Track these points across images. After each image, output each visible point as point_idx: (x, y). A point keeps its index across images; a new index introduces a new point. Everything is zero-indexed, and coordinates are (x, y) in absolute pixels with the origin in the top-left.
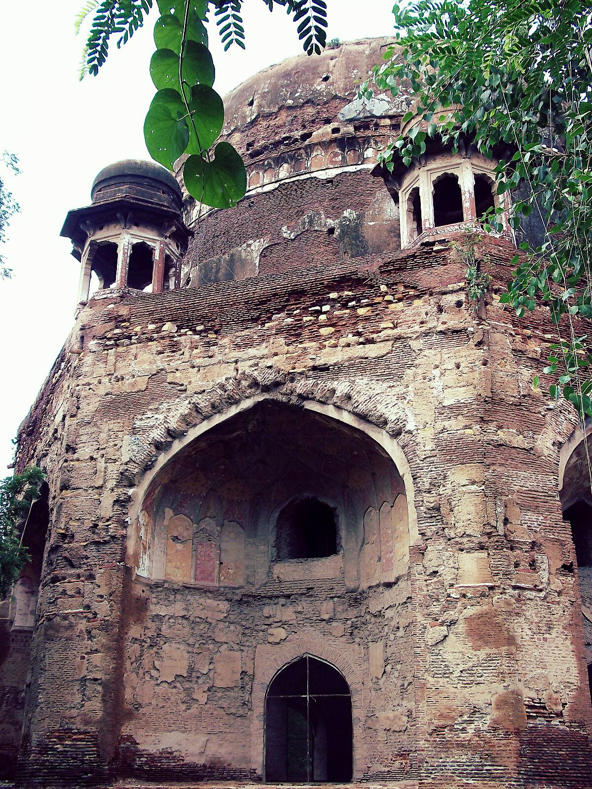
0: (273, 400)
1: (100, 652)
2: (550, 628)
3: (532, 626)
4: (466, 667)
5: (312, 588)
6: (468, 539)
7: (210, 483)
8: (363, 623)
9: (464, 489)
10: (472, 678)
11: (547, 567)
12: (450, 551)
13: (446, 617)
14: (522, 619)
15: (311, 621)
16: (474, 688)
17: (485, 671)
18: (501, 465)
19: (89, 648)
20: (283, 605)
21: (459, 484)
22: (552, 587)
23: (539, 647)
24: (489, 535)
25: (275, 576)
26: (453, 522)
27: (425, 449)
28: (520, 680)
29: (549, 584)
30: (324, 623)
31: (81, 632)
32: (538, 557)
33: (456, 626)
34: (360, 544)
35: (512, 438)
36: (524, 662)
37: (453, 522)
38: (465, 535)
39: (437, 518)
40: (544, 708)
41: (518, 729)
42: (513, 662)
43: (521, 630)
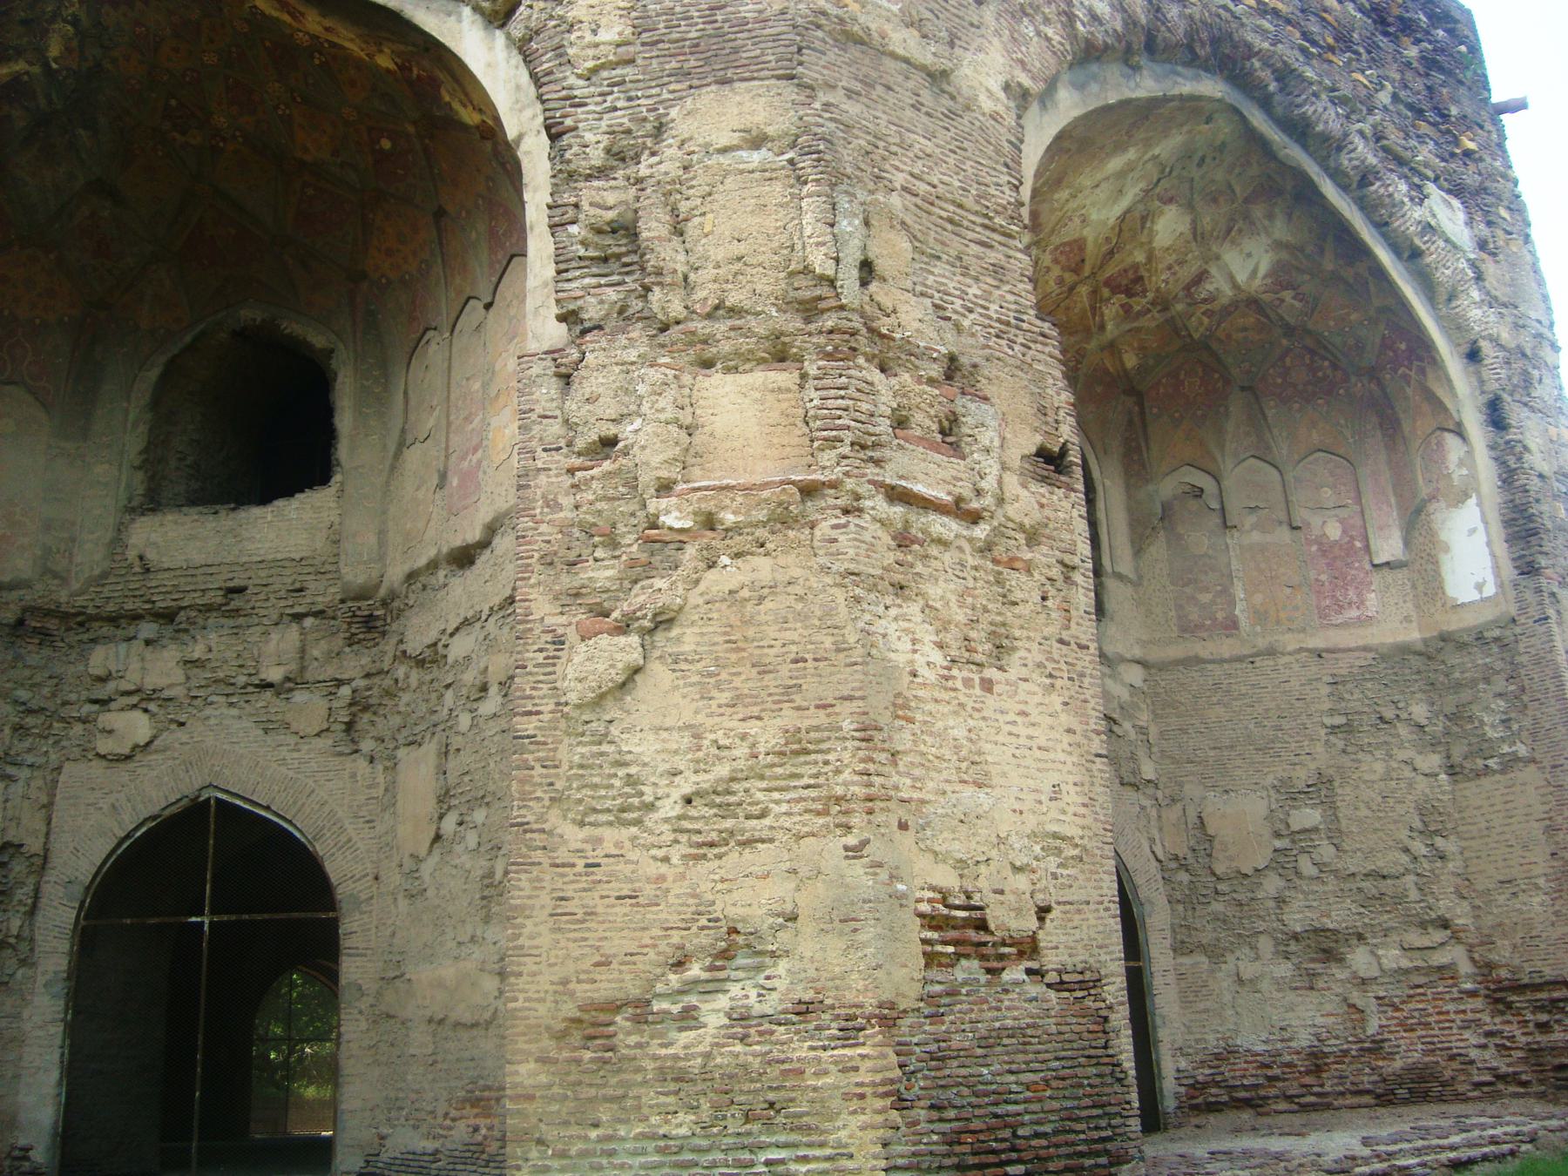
2: (1001, 649)
3: (948, 638)
4: (705, 780)
5: (240, 590)
6: (729, 323)
8: (388, 693)
9: (725, 160)
10: (729, 824)
11: (997, 443)
12: (667, 366)
13: (641, 599)
14: (914, 609)
15: (230, 690)
16: (735, 859)
17: (776, 795)
18: (851, 94)
20: (148, 643)
21: (708, 145)
22: (1011, 510)
23: (969, 708)
24: (809, 310)
25: (132, 554)
26: (681, 268)
27: (597, 39)
28: (903, 826)
29: (1001, 501)
30: (268, 694)
32: (971, 412)
33: (675, 632)
34: (392, 448)
35: (888, 27)
36: (918, 759)
37: (681, 268)
38: (721, 312)
39: (625, 260)
40: (982, 926)
41: (892, 1006)
42: (883, 757)
43: (909, 646)
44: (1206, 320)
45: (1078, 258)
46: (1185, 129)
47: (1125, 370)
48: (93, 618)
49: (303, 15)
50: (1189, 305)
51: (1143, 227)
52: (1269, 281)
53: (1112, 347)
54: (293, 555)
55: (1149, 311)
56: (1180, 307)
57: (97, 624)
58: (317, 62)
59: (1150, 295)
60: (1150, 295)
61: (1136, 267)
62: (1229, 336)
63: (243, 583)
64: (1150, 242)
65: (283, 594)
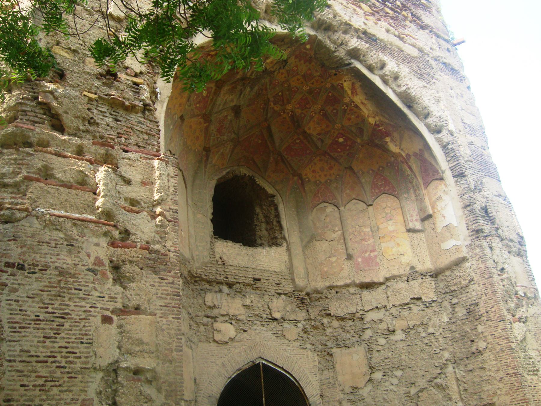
0: (320, 41)
1: (145, 312)
7: (187, 107)
19: (119, 300)
20: (228, 294)
25: (217, 256)
30: (275, 323)
31: (99, 262)
34: (306, 240)
48: (203, 280)
49: (357, 94)
54: (275, 270)
57: (204, 283)
58: (343, 108)
63: (260, 277)
65: (274, 284)
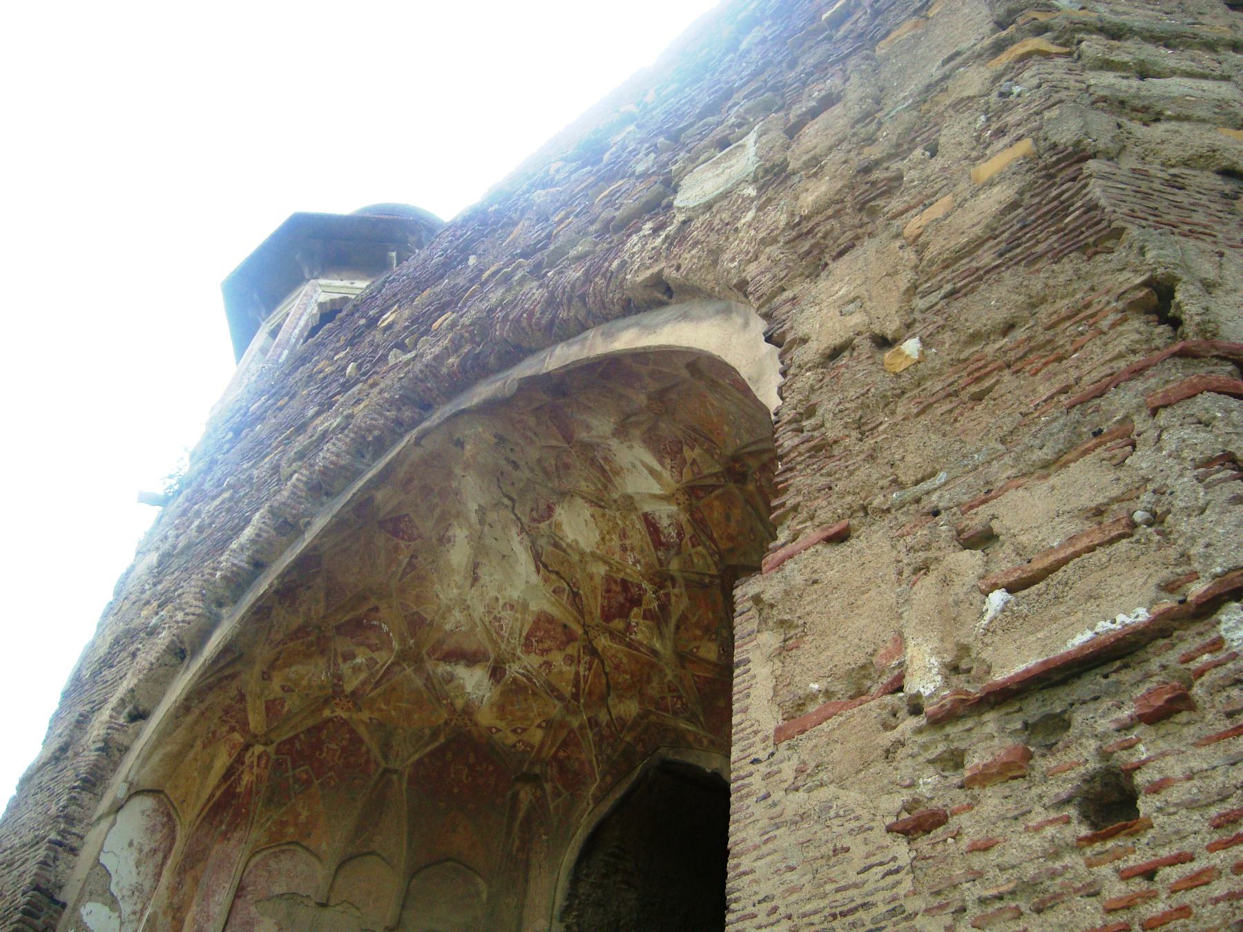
44: (700, 549)
45: (560, 629)
46: (458, 471)
47: (715, 665)
50: (678, 553)
51: (564, 551)
52: (668, 461)
53: (684, 658)
55: (667, 595)
56: (674, 566)
59: (645, 585)
60: (645, 585)
61: (609, 579)
62: (731, 538)
64: (582, 554)
